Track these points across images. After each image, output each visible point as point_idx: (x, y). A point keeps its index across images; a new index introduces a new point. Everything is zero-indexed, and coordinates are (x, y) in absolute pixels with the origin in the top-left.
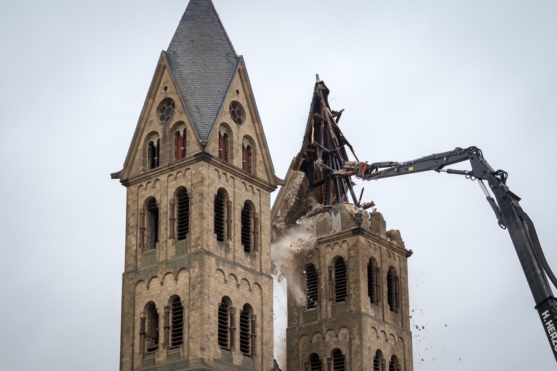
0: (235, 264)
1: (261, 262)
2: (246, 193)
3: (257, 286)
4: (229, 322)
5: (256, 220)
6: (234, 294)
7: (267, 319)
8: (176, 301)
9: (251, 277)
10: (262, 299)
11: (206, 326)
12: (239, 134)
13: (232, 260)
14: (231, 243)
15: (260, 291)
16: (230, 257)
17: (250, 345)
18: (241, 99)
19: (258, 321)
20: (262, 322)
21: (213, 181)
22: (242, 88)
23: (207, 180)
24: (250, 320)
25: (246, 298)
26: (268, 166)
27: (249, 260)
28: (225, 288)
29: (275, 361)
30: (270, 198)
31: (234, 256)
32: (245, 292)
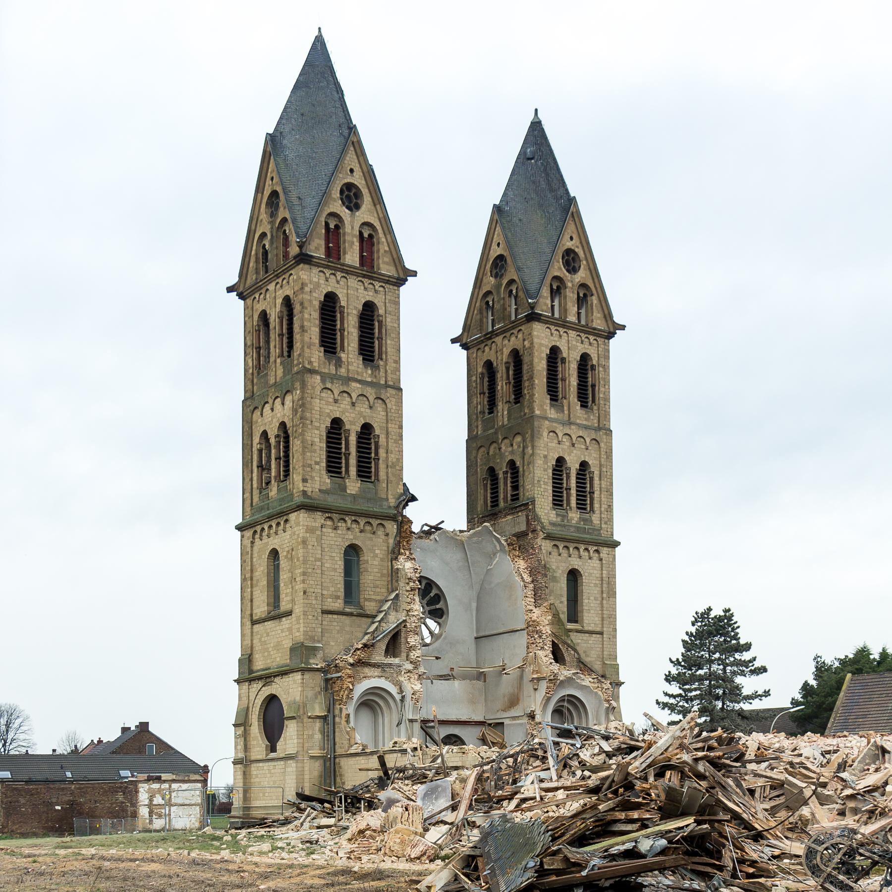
0: (348, 380)
1: (386, 371)
2: (366, 293)
3: (380, 401)
4: (343, 446)
5: (380, 322)
6: (347, 414)
7: (394, 437)
8: (283, 425)
9: (371, 393)
10: (387, 415)
11: (308, 454)
12: (352, 223)
13: (345, 375)
14: (343, 356)
15: (384, 406)
16: (343, 371)
17: (373, 470)
18: (357, 179)
19: (382, 440)
20: (387, 442)
21: (318, 285)
22: (358, 165)
23: (311, 284)
24: (372, 440)
25: (364, 417)
26: (395, 256)
27: (370, 372)
28: (336, 408)
29: (404, 485)
30: (399, 295)
31: (348, 370)
32: (362, 410)
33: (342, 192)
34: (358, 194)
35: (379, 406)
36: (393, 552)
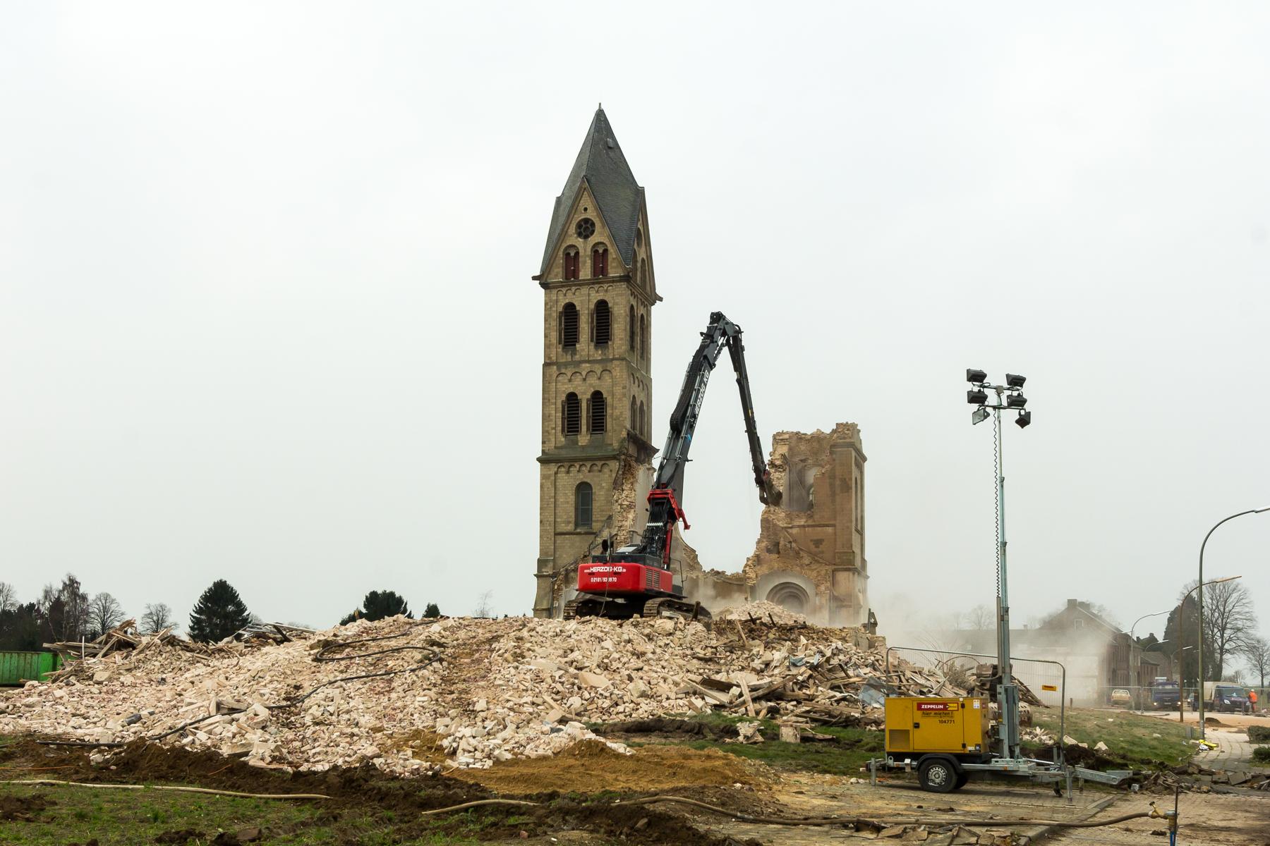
9: (598, 368)
12: (584, 247)
16: (577, 357)
19: (609, 400)
21: (557, 301)
33: (579, 226)
34: (593, 224)
35: (606, 376)
36: (615, 482)
